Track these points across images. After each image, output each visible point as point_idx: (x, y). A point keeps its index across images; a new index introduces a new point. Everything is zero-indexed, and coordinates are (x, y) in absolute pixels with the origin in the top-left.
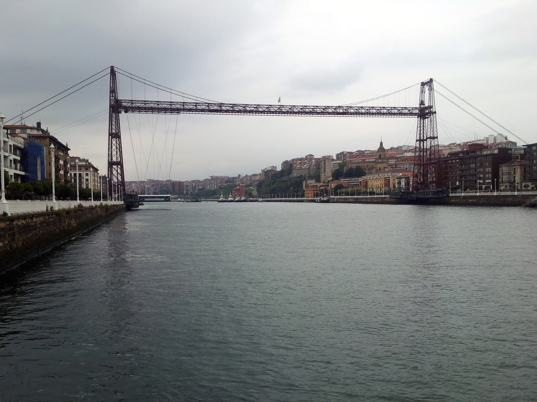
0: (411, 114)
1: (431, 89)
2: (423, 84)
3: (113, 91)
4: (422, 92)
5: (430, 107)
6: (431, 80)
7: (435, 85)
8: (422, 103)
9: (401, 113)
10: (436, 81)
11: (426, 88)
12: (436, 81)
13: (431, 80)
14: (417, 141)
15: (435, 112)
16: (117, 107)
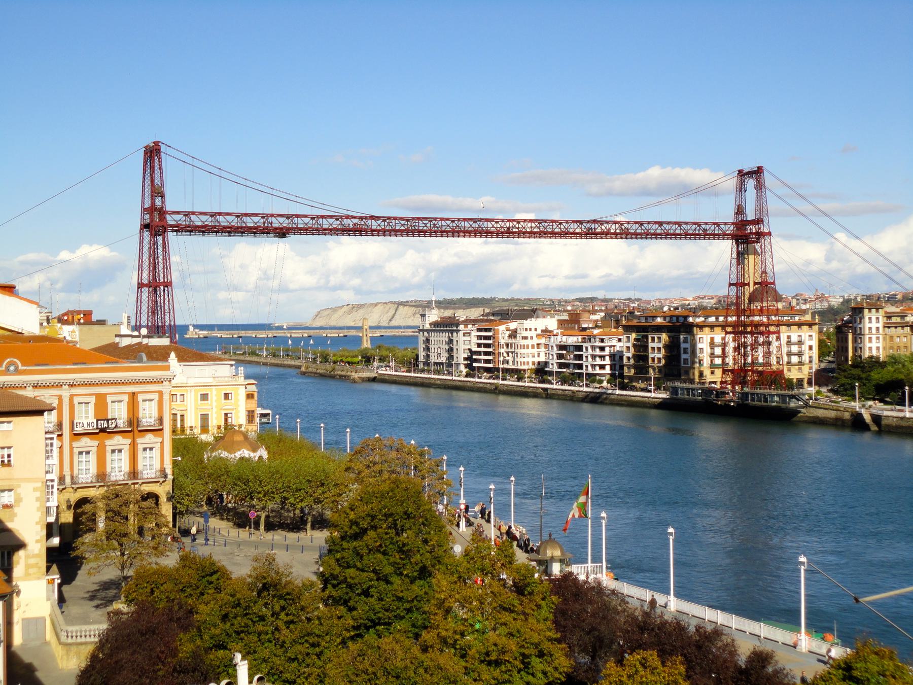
0: (724, 236)
1: (760, 186)
2: (741, 174)
3: (157, 192)
4: (741, 188)
5: (758, 222)
6: (759, 171)
7: (767, 178)
8: (740, 210)
9: (702, 232)
10: (769, 172)
11: (750, 183)
12: (769, 172)
13: (759, 171)
14: (730, 285)
15: (769, 234)
16: (156, 224)
